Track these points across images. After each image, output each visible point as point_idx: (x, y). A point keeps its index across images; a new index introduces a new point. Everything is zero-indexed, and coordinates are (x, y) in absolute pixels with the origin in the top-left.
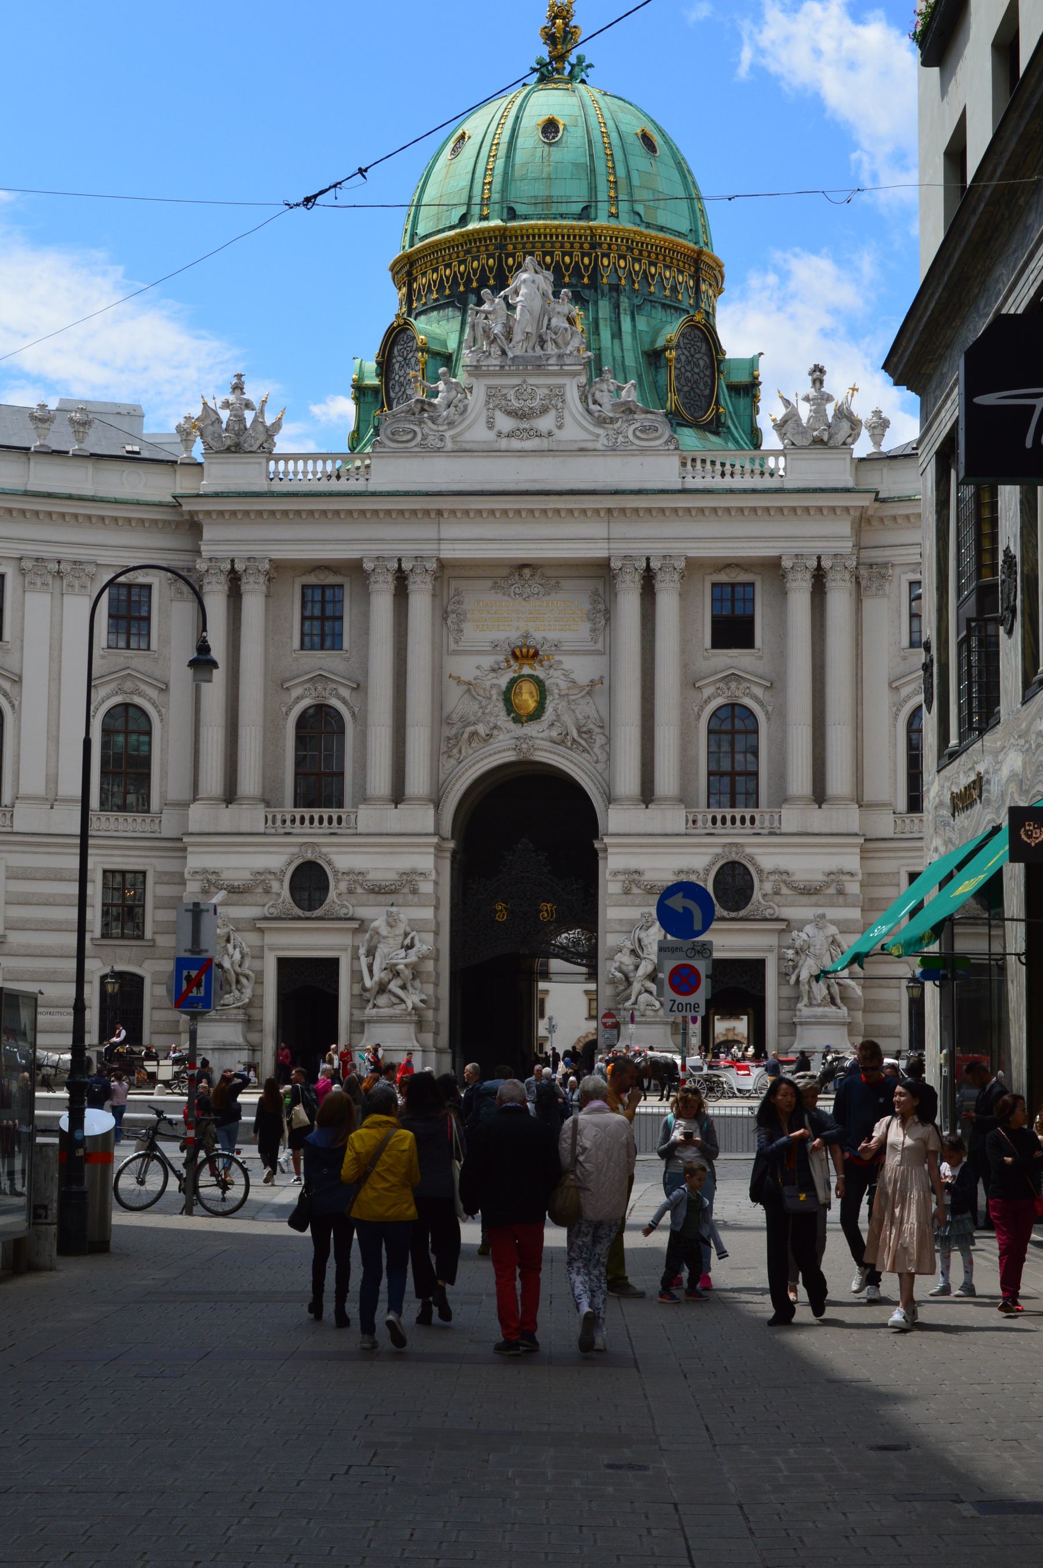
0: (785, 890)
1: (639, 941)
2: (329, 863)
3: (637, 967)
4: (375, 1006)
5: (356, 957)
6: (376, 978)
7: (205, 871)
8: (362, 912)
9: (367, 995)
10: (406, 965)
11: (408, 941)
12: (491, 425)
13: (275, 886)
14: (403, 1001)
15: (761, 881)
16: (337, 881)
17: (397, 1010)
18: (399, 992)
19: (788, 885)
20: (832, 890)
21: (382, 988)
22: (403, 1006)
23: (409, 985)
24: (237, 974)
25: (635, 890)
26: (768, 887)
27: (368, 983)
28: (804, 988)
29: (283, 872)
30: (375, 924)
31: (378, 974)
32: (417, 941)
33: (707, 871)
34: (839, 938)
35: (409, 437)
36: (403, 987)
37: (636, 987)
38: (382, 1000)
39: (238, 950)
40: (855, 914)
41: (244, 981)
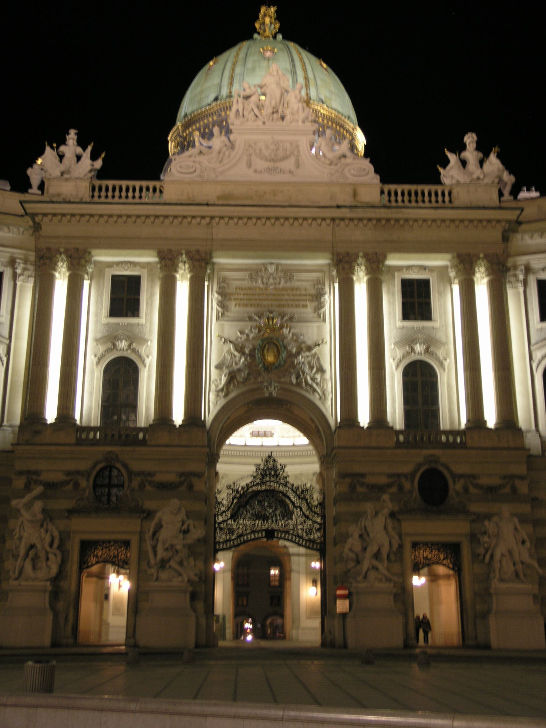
0: (472, 490)
1: (365, 528)
2: (125, 466)
3: (365, 549)
4: (157, 579)
5: (141, 540)
6: (159, 557)
7: (29, 472)
8: (149, 505)
9: (153, 571)
10: (184, 546)
11: (185, 527)
12: (249, 165)
13: (83, 483)
14: (180, 575)
15: (454, 482)
16: (130, 481)
17: (176, 582)
18: (177, 567)
19: (477, 486)
20: (507, 490)
21: (163, 564)
22: (180, 579)
23: (185, 563)
24: (47, 553)
25: (360, 489)
26: (459, 486)
27: (152, 562)
28: (497, 565)
29: (89, 474)
30: (159, 514)
31: (161, 553)
32: (191, 527)
33: (413, 475)
34: (518, 526)
35: (193, 169)
36: (181, 563)
37: (366, 565)
38: (164, 575)
39: (49, 534)
40: (526, 508)
41: (51, 556)
